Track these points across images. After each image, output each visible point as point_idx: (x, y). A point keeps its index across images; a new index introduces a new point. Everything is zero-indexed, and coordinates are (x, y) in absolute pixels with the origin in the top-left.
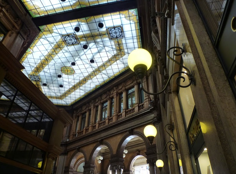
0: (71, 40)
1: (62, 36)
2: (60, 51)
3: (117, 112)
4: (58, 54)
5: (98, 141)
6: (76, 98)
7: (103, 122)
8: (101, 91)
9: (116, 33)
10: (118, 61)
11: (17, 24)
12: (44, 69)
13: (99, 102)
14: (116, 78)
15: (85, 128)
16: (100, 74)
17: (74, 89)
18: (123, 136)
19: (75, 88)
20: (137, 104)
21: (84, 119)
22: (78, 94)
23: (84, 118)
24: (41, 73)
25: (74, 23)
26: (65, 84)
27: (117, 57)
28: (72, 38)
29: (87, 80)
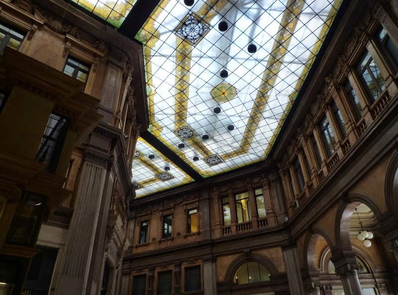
0: (192, 29)
1: (176, 30)
3: (354, 123)
5: (338, 200)
6: (269, 139)
7: (333, 158)
8: (303, 102)
10: (302, 17)
11: (99, 50)
12: (188, 110)
13: (311, 124)
14: (319, 56)
15: (305, 187)
16: (282, 66)
17: (254, 122)
18: (388, 165)
19: (254, 119)
20: (390, 78)
21: (298, 171)
22: (267, 130)
23: (298, 169)
24: (189, 120)
27: (294, 7)
28: (192, 25)
29: (267, 93)
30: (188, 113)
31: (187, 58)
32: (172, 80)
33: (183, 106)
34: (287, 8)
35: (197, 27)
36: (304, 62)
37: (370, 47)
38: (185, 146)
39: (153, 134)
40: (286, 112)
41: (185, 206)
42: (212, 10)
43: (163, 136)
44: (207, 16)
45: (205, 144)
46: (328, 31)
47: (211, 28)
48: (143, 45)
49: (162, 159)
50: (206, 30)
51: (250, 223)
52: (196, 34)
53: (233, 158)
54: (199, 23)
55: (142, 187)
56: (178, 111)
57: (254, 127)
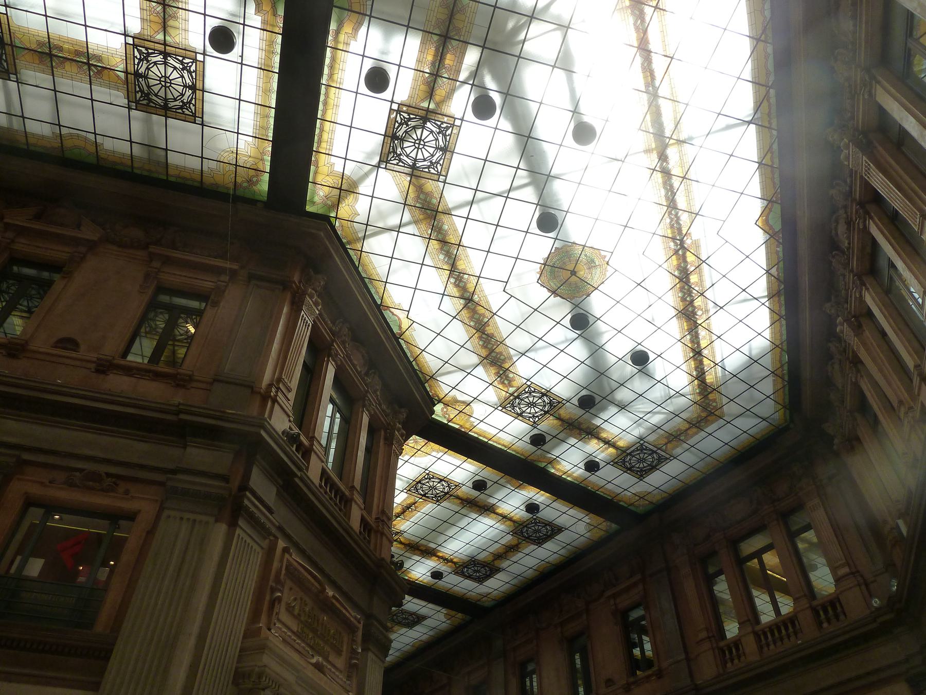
0: (420, 144)
2: (453, 224)
4: (465, 242)
24: (523, 369)
30: (512, 352)
31: (441, 217)
32: (435, 279)
35: (426, 133)
36: (749, 119)
38: (548, 438)
39: (457, 427)
40: (774, 271)
41: (612, 602)
42: (439, 80)
43: (482, 426)
44: (437, 98)
45: (597, 422)
47: (458, 123)
48: (333, 220)
49: (509, 486)
50: (449, 132)
51: (791, 620)
52: (431, 150)
53: (692, 441)
54: (425, 123)
55: (498, 570)
56: (484, 353)
57: (704, 338)
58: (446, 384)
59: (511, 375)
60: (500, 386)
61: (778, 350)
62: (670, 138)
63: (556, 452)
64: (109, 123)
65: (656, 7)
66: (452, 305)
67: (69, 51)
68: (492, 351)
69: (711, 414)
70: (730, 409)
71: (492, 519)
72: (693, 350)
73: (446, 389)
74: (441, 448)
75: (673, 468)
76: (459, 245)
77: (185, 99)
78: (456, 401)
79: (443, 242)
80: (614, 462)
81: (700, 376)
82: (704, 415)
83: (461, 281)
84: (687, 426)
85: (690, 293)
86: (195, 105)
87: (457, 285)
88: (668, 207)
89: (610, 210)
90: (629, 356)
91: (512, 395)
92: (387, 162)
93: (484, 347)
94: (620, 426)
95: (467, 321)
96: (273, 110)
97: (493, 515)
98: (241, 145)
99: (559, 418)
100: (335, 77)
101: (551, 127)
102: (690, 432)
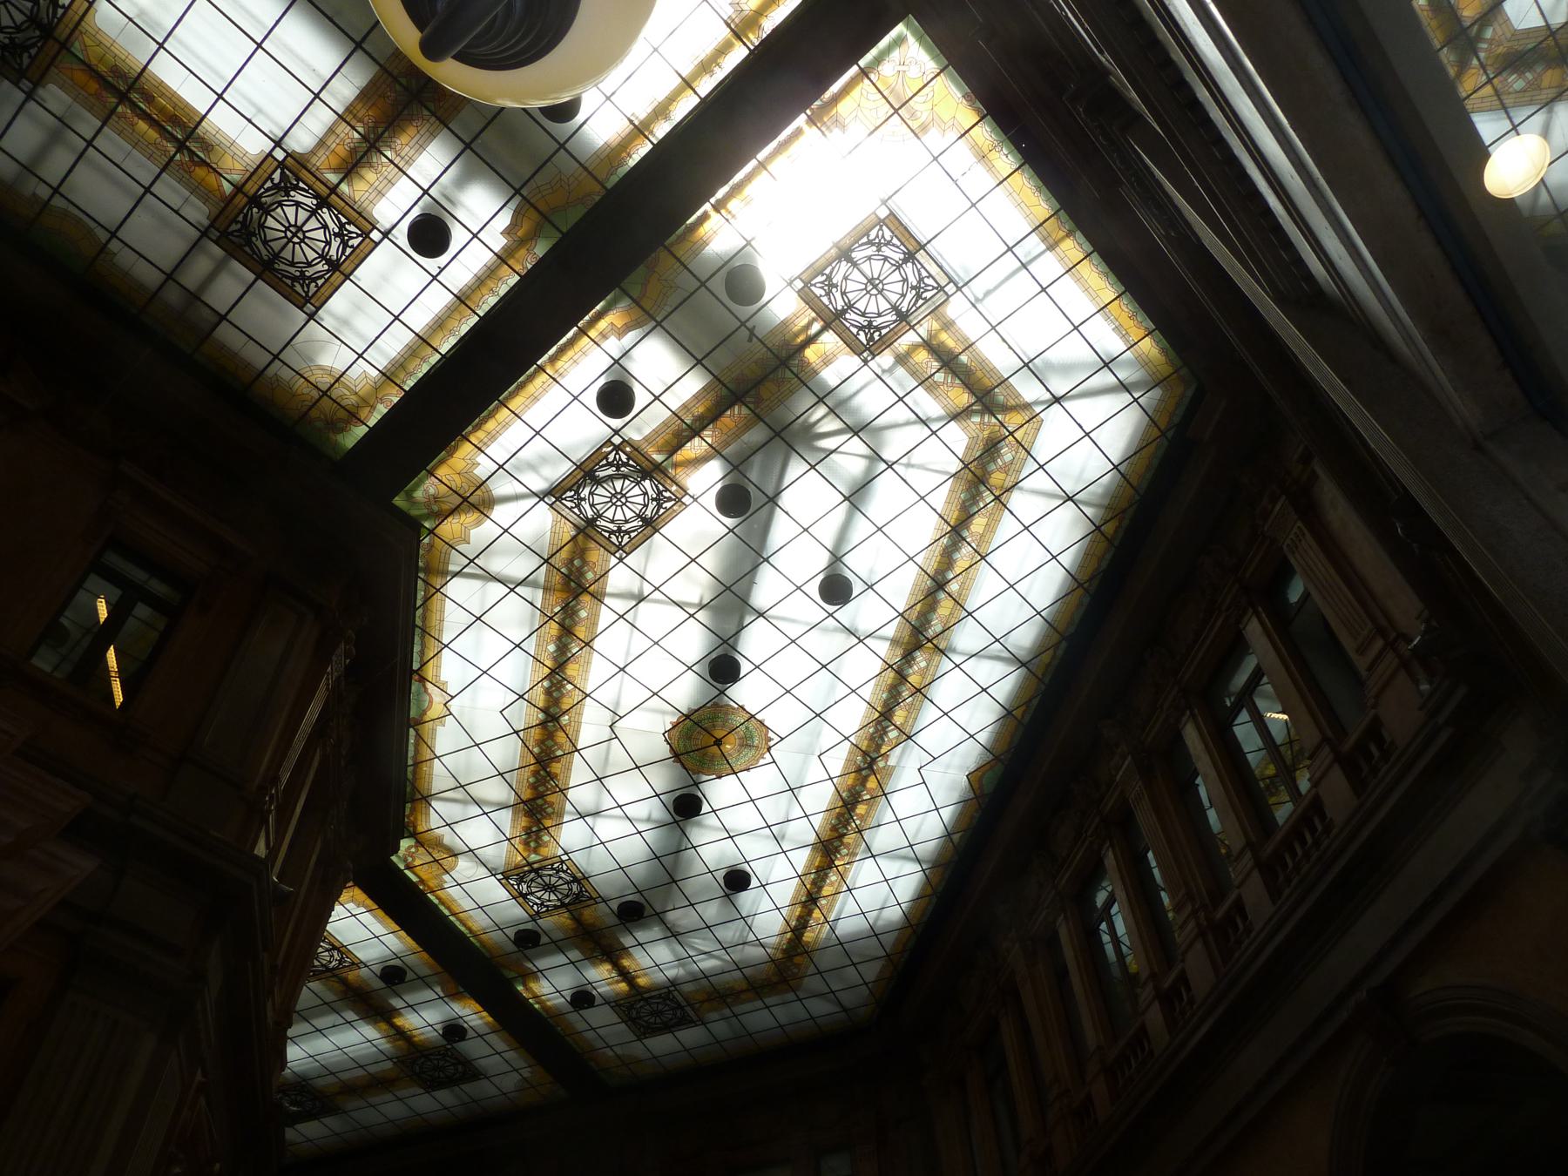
0: (618, 498)
1: (555, 493)
4: (596, 644)
9: (874, 285)
10: (1016, 500)
12: (571, 794)
20: (1327, 749)
24: (570, 836)
25: (583, 364)
26: (754, 851)
28: (618, 484)
29: (885, 756)
30: (568, 807)
31: (586, 598)
32: (520, 672)
33: (552, 776)
34: (966, 466)
36: (1025, 660)
37: (1253, 629)
38: (544, 939)
39: (414, 879)
40: (956, 837)
43: (455, 892)
44: (678, 457)
45: (627, 941)
46: (1108, 557)
49: (438, 989)
50: (668, 505)
52: (629, 514)
53: (738, 1009)
57: (832, 884)
58: (438, 816)
59: (546, 838)
60: (520, 848)
61: (909, 931)
62: (930, 641)
63: (542, 963)
64: (154, 232)
65: (997, 498)
66: (524, 716)
67: (162, 110)
68: (542, 796)
69: (784, 981)
70: (813, 983)
71: (379, 1031)
72: (809, 893)
73: (434, 821)
74: (369, 902)
75: (691, 1036)
76: (587, 644)
77: (310, 272)
78: (439, 844)
79: (567, 631)
80: (615, 1003)
81: (798, 928)
82: (775, 979)
83: (559, 689)
84: (744, 986)
85: (846, 824)
86: (319, 288)
87: (548, 692)
88: (881, 714)
89: (805, 684)
90: (723, 872)
91: (529, 864)
92: (559, 499)
93: (534, 787)
94: (654, 959)
95: (531, 744)
96: (438, 357)
97: (384, 1026)
98: (354, 373)
99: (577, 920)
100: (559, 364)
101: (794, 557)
102: (743, 996)
